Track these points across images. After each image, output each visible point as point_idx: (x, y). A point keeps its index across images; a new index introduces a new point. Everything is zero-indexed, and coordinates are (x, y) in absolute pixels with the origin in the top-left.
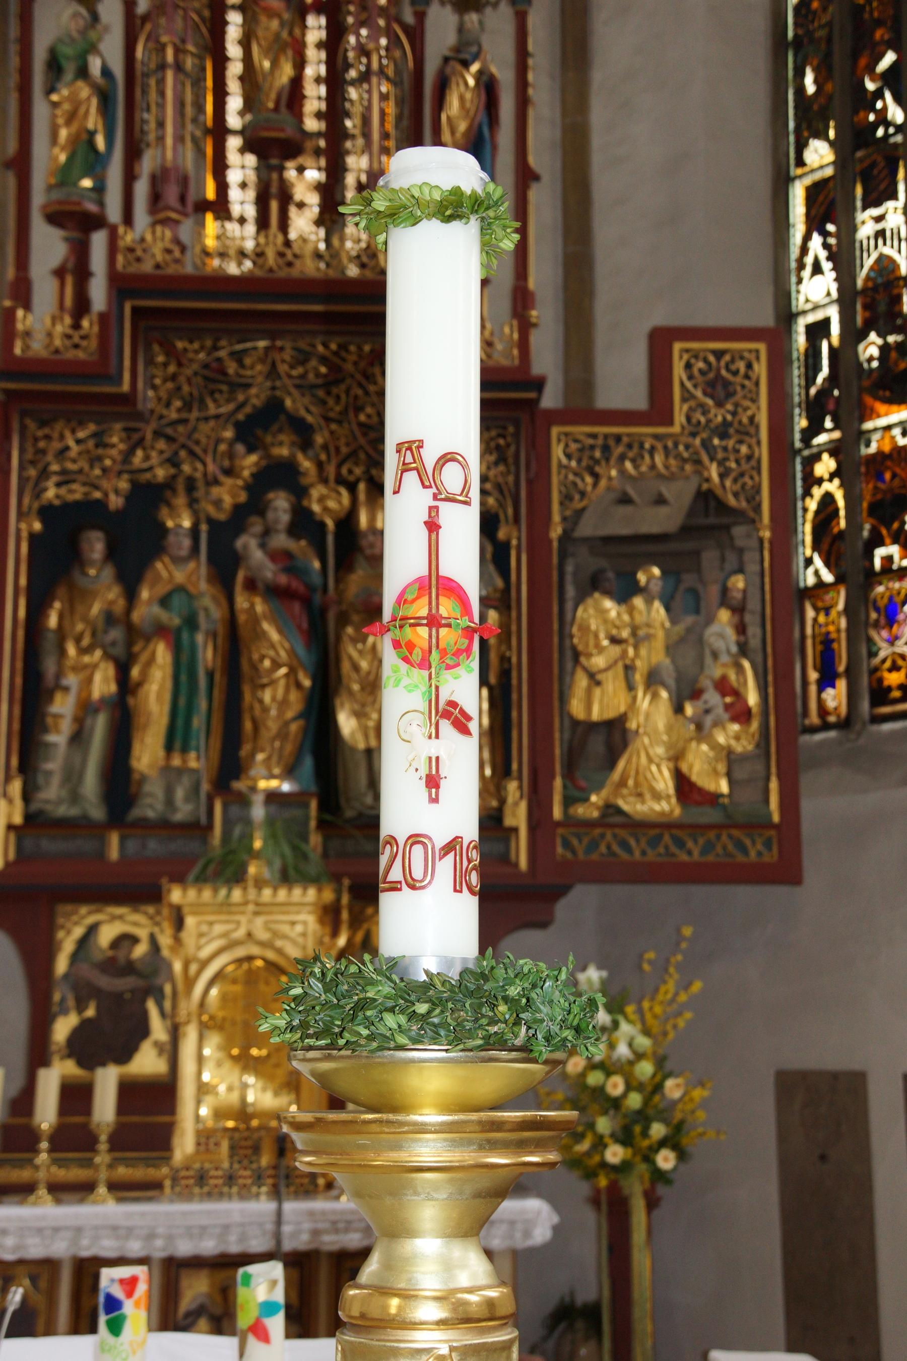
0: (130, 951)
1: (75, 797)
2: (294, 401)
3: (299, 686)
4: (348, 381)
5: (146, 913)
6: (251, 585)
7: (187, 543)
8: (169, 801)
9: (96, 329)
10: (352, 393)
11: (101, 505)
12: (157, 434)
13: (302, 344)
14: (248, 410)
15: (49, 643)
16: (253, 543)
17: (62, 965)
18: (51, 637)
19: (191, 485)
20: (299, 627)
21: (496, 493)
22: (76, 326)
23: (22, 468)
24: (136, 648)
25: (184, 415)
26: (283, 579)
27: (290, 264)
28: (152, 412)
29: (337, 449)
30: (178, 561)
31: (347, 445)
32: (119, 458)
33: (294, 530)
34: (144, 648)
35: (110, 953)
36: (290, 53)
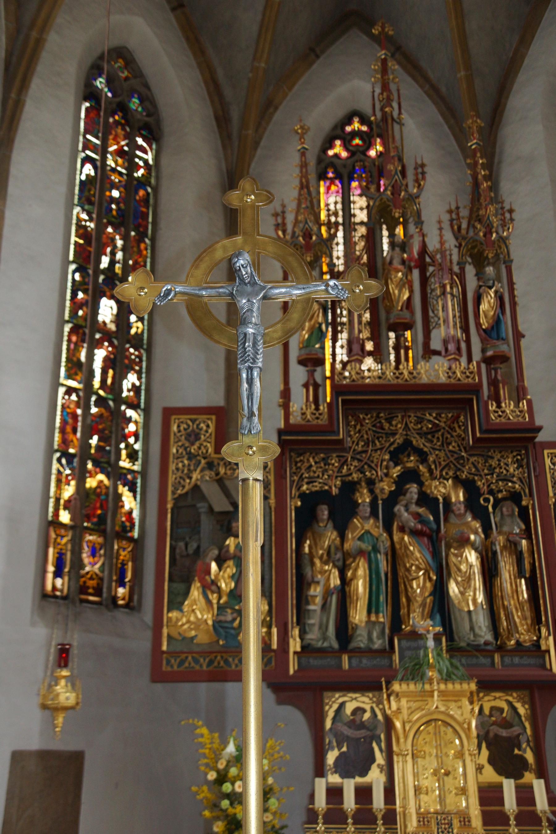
0: (362, 717)
1: (325, 638)
2: (417, 441)
3: (430, 579)
4: (442, 431)
5: (368, 697)
6: (402, 529)
7: (368, 510)
8: (370, 639)
9: (326, 410)
10: (445, 436)
11: (328, 492)
12: (353, 458)
13: (419, 414)
14: (395, 445)
15: (306, 561)
16: (402, 509)
17: (328, 724)
18: (307, 556)
19: (371, 483)
20: (428, 549)
21: (519, 483)
22: (317, 409)
23: (291, 476)
24: (348, 562)
25: (365, 449)
26: (419, 526)
27: (414, 378)
28: (350, 448)
29: (440, 463)
30: (367, 519)
31: (444, 461)
32: (336, 470)
33: (419, 503)
34: (354, 561)
35: (352, 718)
36: (407, 286)
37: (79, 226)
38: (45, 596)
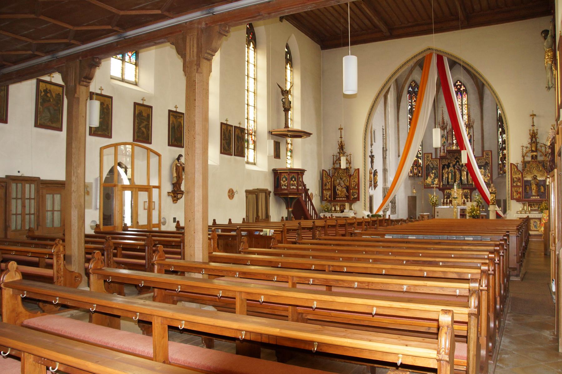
37: (409, 118)
38: (409, 176)
